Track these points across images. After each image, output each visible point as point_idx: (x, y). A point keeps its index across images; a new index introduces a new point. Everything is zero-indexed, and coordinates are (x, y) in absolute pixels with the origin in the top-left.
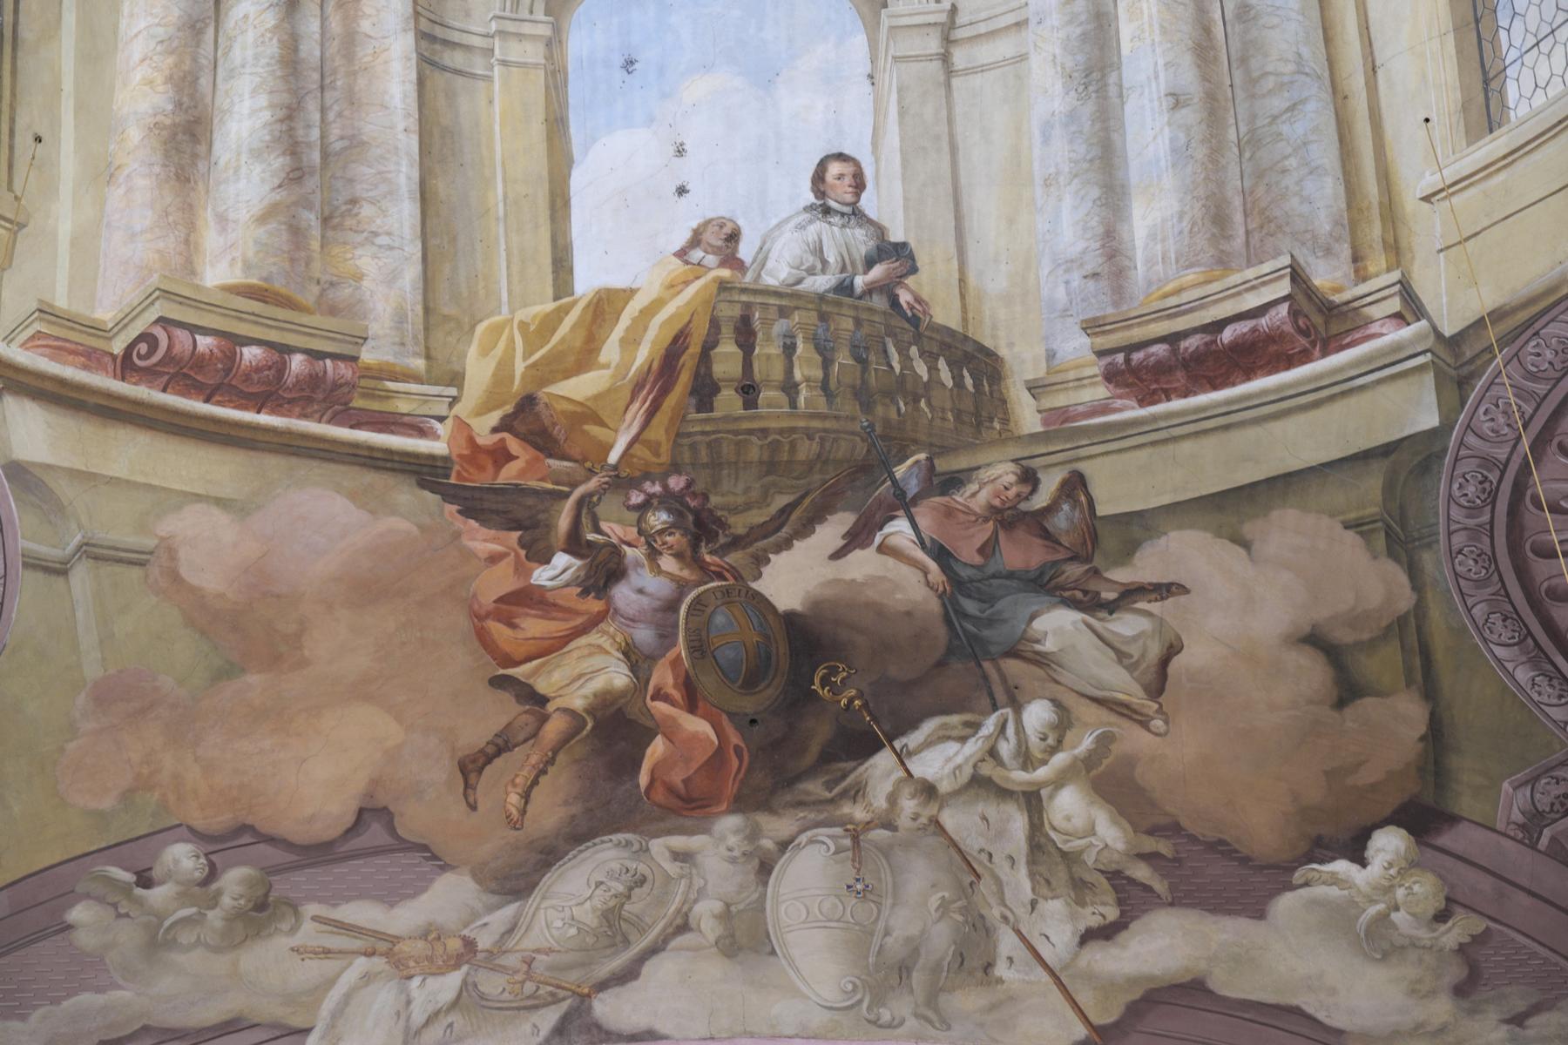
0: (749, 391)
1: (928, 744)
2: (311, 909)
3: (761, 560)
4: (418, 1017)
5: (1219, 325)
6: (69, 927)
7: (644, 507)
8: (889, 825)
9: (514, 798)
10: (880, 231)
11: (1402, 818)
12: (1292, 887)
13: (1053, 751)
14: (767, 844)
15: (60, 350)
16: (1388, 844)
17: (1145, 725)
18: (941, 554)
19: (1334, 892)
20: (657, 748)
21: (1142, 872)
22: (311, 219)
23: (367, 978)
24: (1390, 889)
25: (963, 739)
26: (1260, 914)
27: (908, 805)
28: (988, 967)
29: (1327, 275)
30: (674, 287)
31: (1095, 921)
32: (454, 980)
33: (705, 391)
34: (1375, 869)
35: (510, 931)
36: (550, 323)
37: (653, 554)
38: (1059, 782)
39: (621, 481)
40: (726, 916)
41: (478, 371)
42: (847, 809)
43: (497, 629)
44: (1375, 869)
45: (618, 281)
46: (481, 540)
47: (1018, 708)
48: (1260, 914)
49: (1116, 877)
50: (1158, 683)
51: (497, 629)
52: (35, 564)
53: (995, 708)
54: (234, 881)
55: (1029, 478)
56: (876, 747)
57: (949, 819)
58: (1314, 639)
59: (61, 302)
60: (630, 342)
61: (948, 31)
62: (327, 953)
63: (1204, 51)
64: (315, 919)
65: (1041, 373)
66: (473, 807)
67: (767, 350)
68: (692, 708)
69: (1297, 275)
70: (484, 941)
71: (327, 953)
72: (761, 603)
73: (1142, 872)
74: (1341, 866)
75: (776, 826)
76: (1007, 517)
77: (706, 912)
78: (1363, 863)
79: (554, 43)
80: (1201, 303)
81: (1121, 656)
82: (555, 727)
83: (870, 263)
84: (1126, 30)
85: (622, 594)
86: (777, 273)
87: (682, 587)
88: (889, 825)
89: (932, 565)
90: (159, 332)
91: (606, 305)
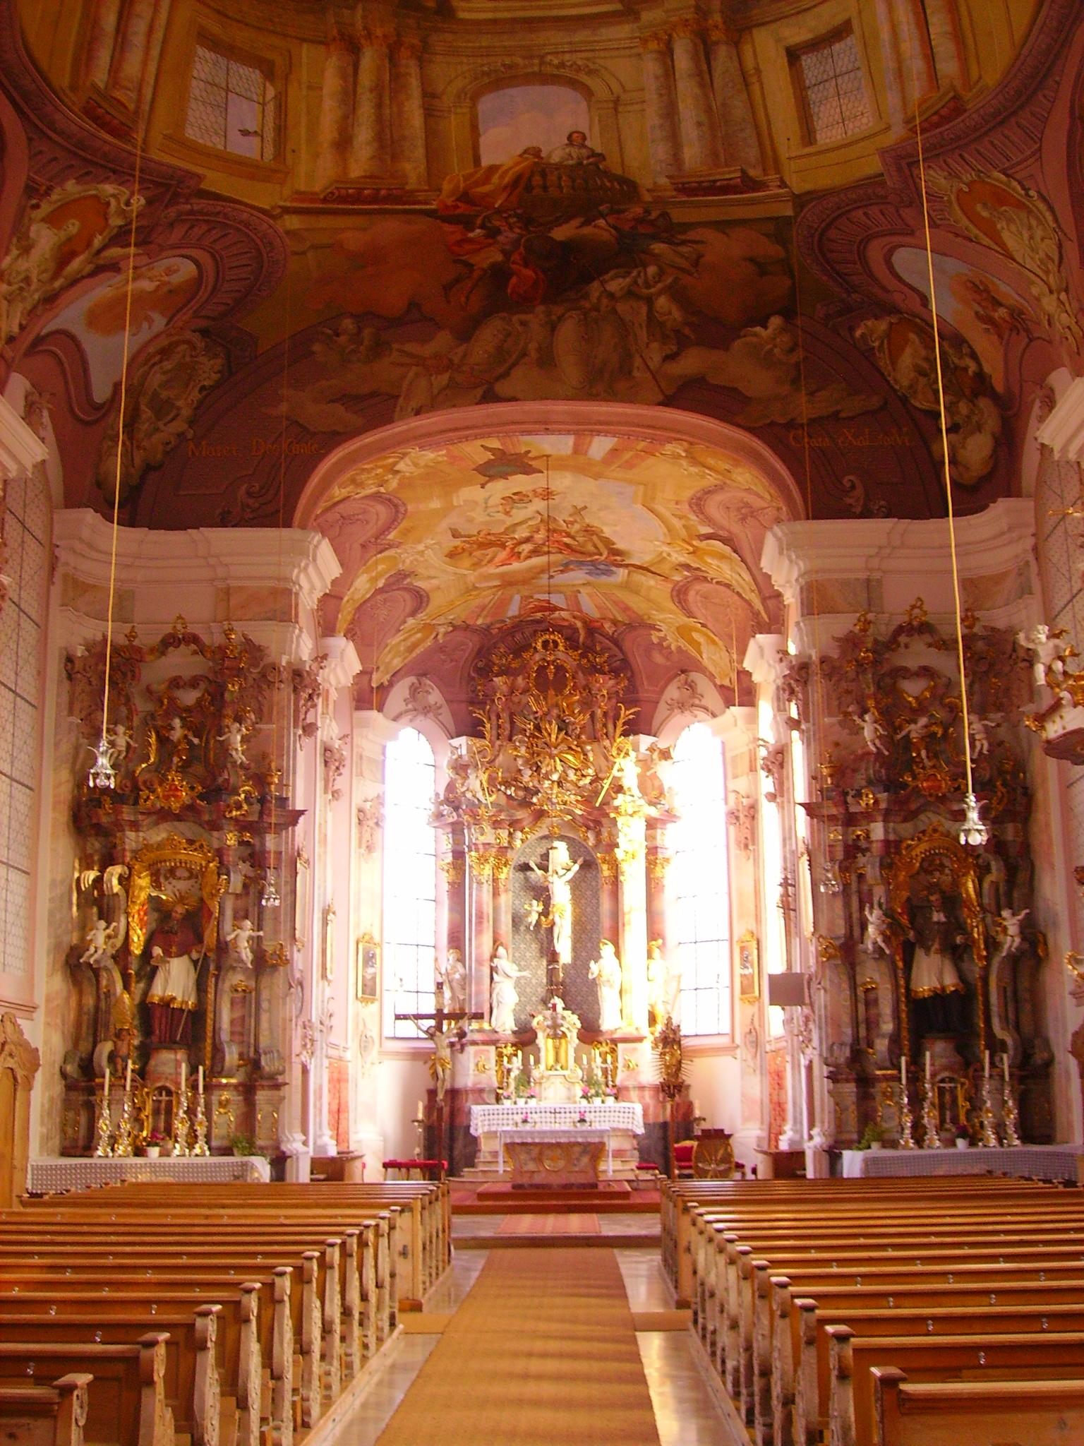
0: (545, 188)
1: (612, 279)
2: (395, 346)
3: (550, 229)
4: (435, 391)
5: (715, 181)
6: (314, 353)
7: (510, 216)
8: (598, 310)
9: (463, 299)
10: (592, 150)
11: (778, 313)
12: (739, 337)
13: (656, 283)
14: (554, 317)
15: (302, 201)
16: (775, 321)
17: (690, 274)
18: (615, 228)
19: (754, 339)
20: (514, 280)
21: (687, 331)
22: (388, 158)
23: (417, 375)
24: (774, 339)
25: (624, 277)
26: (727, 349)
27: (605, 301)
28: (630, 373)
29: (752, 173)
30: (518, 164)
31: (669, 352)
32: (446, 376)
33: (529, 188)
34: (770, 330)
35: (465, 355)
36: (471, 175)
37: (511, 228)
38: (659, 294)
39: (499, 211)
40: (539, 349)
41: (447, 187)
42: (583, 302)
43: (456, 249)
44: (770, 330)
45: (498, 163)
46: (447, 228)
47: (645, 266)
48: (727, 349)
49: (677, 332)
50: (696, 264)
51: (456, 249)
52: (296, 253)
53: (637, 267)
54: (367, 333)
55: (647, 212)
56: (593, 279)
57: (621, 308)
58: (751, 260)
59: (302, 188)
60: (502, 177)
61: (617, 101)
62: (402, 365)
63: (709, 110)
64: (398, 350)
65: (651, 186)
66: (449, 302)
67: (552, 178)
68: (526, 265)
69: (743, 171)
70: (456, 361)
71: (402, 365)
72: (551, 238)
73: (687, 331)
74: (758, 329)
75: (558, 310)
76: (639, 221)
77: (532, 346)
78: (765, 327)
79: (473, 106)
80: (710, 175)
81: (682, 256)
82: (476, 274)
83: (588, 158)
84: (681, 106)
85: (501, 238)
86: (555, 158)
87: (522, 236)
88: (598, 310)
89: (613, 231)
90: (337, 193)
91: (493, 169)
